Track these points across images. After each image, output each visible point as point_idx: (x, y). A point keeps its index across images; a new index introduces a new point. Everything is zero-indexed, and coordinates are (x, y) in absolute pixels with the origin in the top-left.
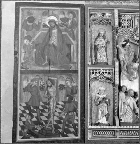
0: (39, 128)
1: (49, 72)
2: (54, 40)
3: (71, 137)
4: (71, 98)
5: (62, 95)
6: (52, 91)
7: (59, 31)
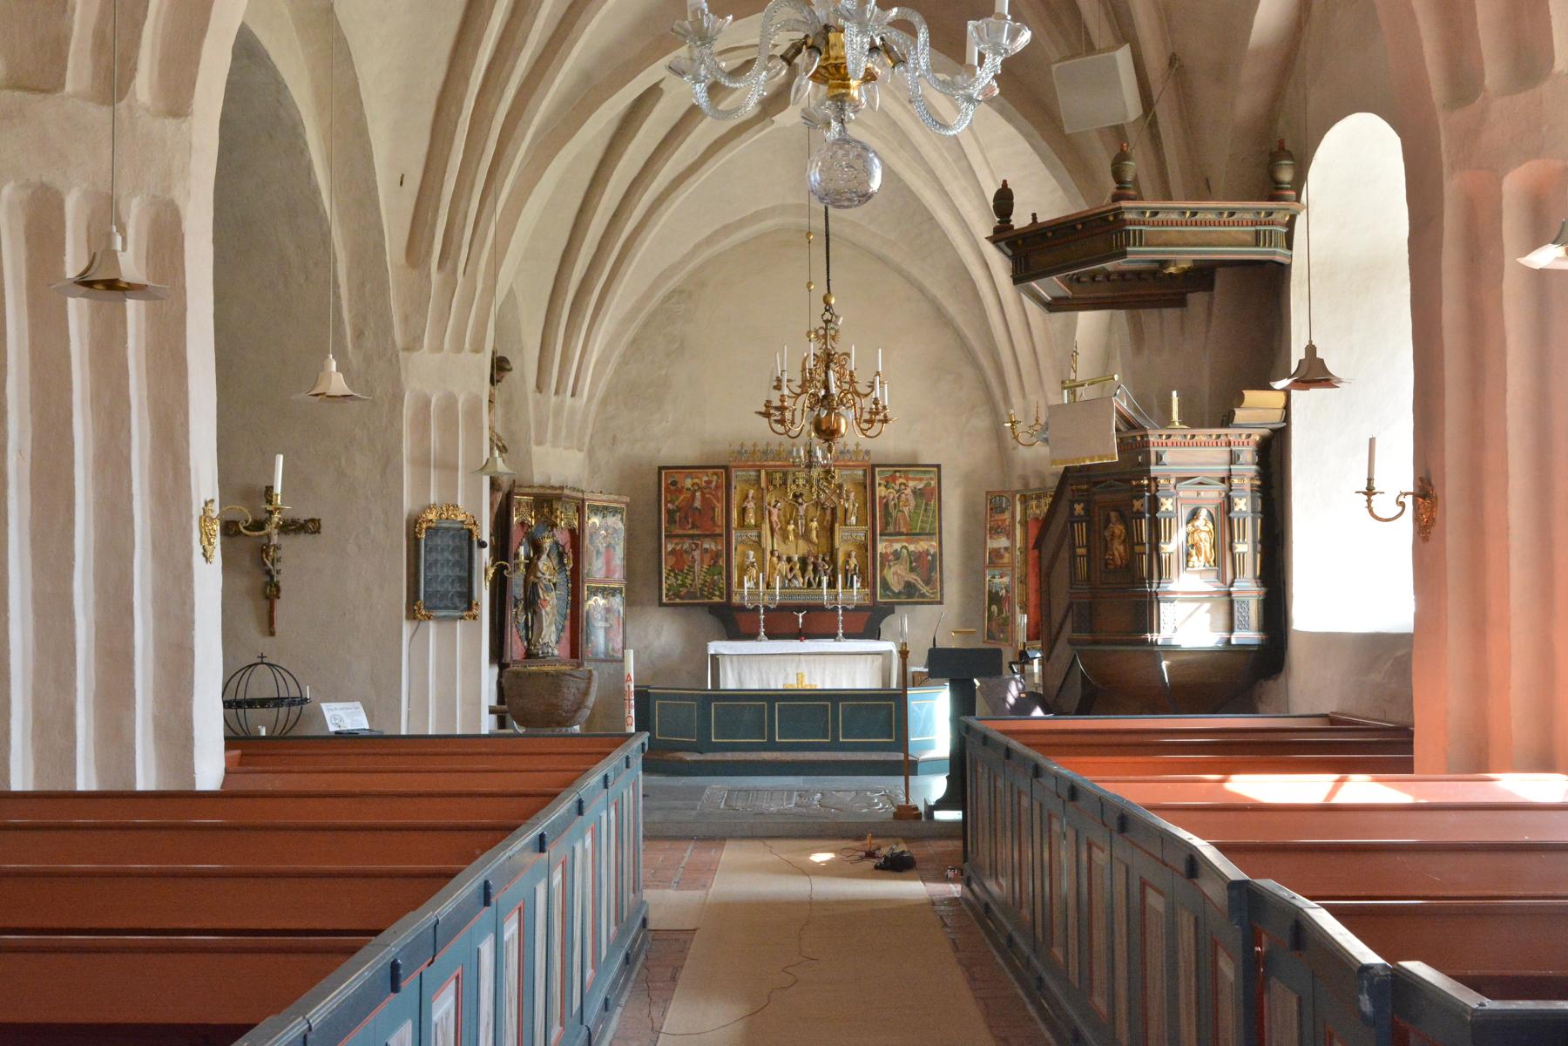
0: (684, 591)
1: (692, 537)
2: (697, 504)
3: (716, 599)
4: (716, 562)
5: (707, 557)
6: (697, 554)
7: (703, 495)
